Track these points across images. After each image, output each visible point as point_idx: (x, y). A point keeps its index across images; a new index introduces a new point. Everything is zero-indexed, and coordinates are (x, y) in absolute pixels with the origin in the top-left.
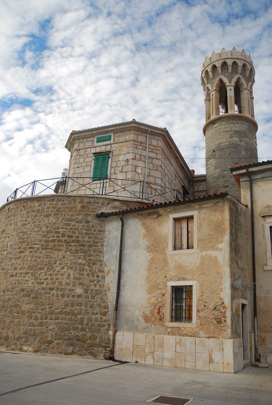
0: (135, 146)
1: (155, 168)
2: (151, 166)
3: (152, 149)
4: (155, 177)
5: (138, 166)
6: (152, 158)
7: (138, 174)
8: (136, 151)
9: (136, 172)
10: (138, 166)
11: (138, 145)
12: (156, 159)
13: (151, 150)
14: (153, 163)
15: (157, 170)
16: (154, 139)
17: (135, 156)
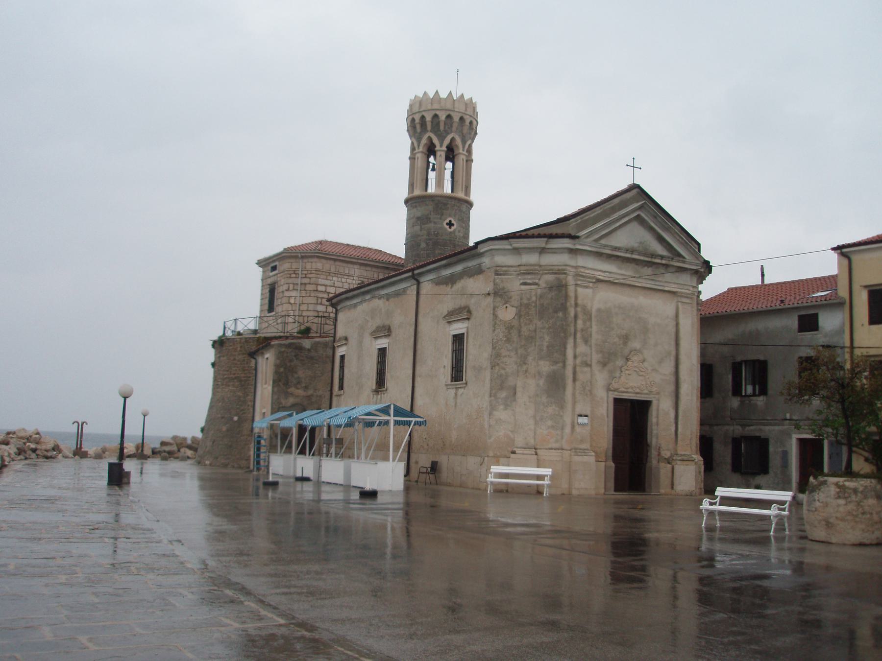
0: (289, 276)
1: (308, 295)
2: (303, 293)
3: (306, 274)
4: (308, 304)
5: (291, 297)
6: (305, 284)
7: (291, 304)
8: (290, 281)
9: (289, 303)
10: (291, 297)
11: (292, 274)
12: (310, 284)
13: (304, 276)
14: (306, 289)
15: (310, 296)
16: (308, 262)
17: (289, 287)
